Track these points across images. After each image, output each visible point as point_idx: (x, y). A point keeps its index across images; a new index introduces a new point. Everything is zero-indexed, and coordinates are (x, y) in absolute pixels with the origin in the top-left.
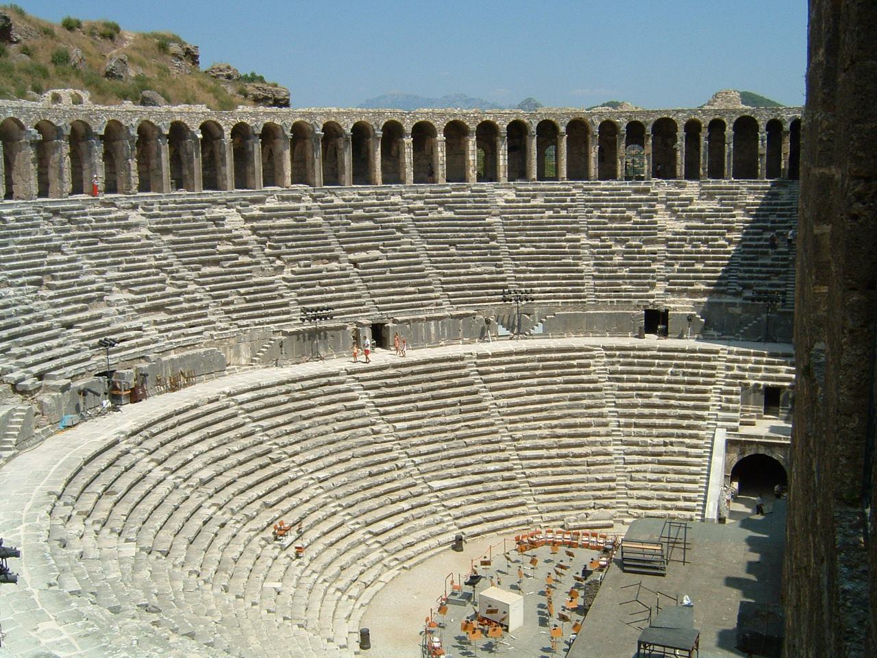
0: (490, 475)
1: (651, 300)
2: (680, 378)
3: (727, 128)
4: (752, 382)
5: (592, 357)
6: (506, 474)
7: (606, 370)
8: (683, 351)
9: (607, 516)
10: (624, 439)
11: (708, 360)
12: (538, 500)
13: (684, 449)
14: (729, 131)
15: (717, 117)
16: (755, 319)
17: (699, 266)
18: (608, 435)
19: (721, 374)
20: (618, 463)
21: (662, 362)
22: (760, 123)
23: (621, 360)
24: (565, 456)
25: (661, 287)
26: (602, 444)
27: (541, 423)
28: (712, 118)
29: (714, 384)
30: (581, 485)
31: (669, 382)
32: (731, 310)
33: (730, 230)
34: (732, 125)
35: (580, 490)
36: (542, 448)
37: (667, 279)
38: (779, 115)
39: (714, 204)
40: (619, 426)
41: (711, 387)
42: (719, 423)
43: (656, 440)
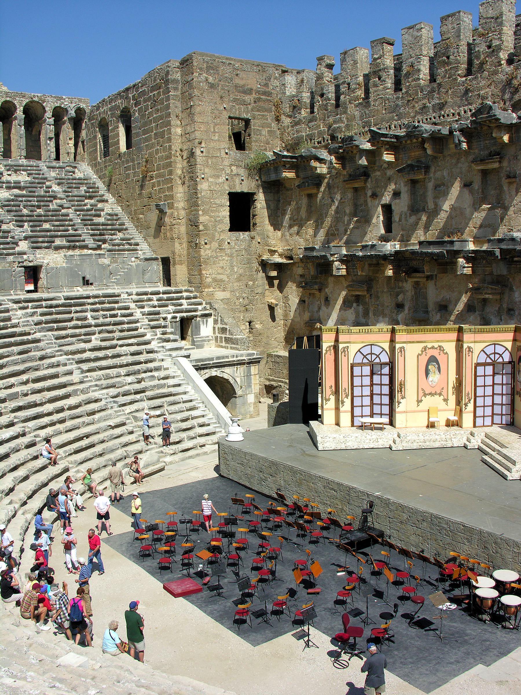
0: (12, 444)
1: (25, 257)
2: (101, 321)
3: (18, 111)
4: (169, 316)
5: (7, 311)
6: (25, 440)
7: (28, 321)
8: (88, 297)
9: (155, 458)
10: (98, 383)
11: (117, 302)
12: (75, 462)
13: (156, 382)
14: (19, 113)
15: (8, 99)
16: (124, 269)
17: (46, 226)
18: (81, 382)
19: (138, 314)
20: (112, 407)
21: (78, 308)
22: (47, 109)
23: (39, 310)
24: (61, 410)
25: (23, 246)
26: (83, 392)
27: (12, 380)
28: (3, 100)
29: (137, 322)
30: (101, 436)
31: (97, 326)
32: (102, 261)
33: (55, 198)
34: (22, 108)
35: (103, 442)
36: (35, 405)
37: (26, 238)
38: (63, 103)
39: (23, 178)
40: (83, 372)
41: (138, 325)
42: (174, 354)
43: (129, 379)
